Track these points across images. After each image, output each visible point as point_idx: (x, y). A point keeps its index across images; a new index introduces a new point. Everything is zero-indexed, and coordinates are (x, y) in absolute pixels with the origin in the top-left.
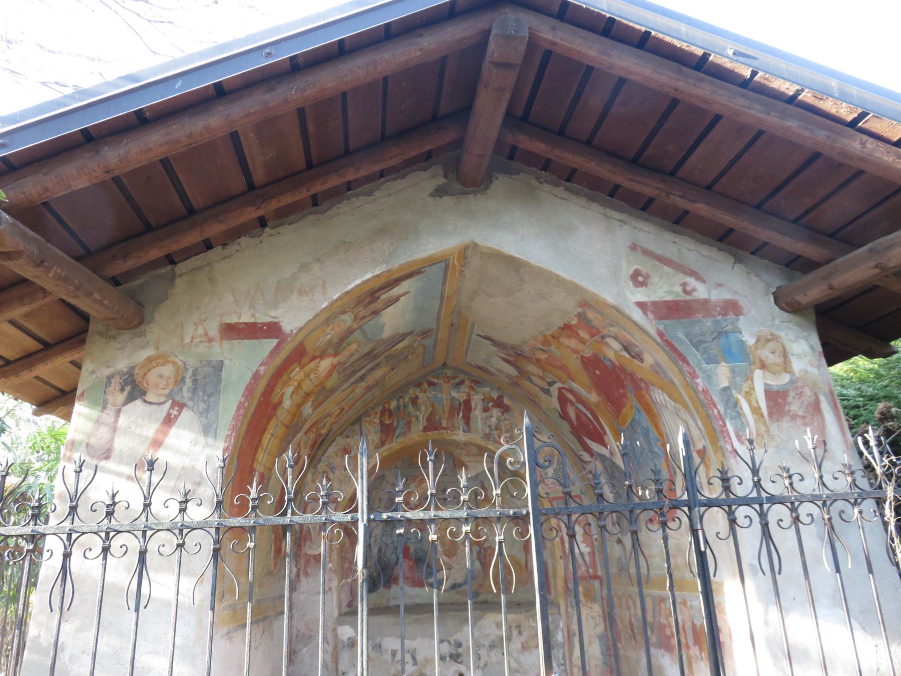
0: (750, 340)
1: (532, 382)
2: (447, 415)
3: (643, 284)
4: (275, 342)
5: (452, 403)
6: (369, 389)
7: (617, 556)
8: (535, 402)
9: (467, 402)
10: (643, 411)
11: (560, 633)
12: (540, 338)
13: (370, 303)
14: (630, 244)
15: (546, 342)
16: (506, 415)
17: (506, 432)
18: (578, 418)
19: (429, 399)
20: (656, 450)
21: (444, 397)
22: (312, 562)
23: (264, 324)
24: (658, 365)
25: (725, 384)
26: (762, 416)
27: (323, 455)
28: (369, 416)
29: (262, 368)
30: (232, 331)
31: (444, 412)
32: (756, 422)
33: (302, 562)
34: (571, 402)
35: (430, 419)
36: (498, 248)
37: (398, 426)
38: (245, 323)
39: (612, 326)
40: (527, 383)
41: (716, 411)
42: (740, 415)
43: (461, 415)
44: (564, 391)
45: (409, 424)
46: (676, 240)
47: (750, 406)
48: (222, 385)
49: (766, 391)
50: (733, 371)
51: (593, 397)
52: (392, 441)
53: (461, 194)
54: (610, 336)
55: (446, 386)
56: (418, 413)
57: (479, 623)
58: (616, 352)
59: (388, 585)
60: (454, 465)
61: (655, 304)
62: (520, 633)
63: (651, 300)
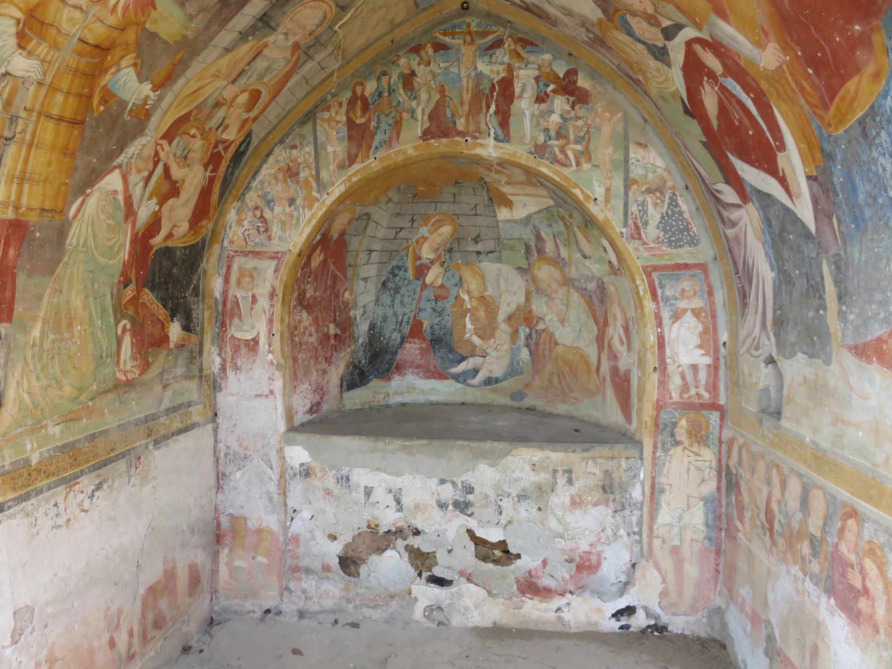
1: (630, 33)
2: (466, 107)
5: (478, 85)
6: (302, 52)
7: (761, 385)
8: (637, 82)
11: (638, 487)
16: (581, 111)
17: (577, 142)
19: (434, 76)
21: (463, 74)
22: (244, 350)
27: (253, 178)
28: (328, 109)
33: (228, 349)
34: (711, 75)
35: (435, 115)
37: (378, 127)
43: (493, 108)
44: (697, 48)
45: (397, 124)
51: (768, 57)
55: (468, 51)
57: (504, 461)
59: (385, 374)
60: (491, 199)
62: (570, 481)
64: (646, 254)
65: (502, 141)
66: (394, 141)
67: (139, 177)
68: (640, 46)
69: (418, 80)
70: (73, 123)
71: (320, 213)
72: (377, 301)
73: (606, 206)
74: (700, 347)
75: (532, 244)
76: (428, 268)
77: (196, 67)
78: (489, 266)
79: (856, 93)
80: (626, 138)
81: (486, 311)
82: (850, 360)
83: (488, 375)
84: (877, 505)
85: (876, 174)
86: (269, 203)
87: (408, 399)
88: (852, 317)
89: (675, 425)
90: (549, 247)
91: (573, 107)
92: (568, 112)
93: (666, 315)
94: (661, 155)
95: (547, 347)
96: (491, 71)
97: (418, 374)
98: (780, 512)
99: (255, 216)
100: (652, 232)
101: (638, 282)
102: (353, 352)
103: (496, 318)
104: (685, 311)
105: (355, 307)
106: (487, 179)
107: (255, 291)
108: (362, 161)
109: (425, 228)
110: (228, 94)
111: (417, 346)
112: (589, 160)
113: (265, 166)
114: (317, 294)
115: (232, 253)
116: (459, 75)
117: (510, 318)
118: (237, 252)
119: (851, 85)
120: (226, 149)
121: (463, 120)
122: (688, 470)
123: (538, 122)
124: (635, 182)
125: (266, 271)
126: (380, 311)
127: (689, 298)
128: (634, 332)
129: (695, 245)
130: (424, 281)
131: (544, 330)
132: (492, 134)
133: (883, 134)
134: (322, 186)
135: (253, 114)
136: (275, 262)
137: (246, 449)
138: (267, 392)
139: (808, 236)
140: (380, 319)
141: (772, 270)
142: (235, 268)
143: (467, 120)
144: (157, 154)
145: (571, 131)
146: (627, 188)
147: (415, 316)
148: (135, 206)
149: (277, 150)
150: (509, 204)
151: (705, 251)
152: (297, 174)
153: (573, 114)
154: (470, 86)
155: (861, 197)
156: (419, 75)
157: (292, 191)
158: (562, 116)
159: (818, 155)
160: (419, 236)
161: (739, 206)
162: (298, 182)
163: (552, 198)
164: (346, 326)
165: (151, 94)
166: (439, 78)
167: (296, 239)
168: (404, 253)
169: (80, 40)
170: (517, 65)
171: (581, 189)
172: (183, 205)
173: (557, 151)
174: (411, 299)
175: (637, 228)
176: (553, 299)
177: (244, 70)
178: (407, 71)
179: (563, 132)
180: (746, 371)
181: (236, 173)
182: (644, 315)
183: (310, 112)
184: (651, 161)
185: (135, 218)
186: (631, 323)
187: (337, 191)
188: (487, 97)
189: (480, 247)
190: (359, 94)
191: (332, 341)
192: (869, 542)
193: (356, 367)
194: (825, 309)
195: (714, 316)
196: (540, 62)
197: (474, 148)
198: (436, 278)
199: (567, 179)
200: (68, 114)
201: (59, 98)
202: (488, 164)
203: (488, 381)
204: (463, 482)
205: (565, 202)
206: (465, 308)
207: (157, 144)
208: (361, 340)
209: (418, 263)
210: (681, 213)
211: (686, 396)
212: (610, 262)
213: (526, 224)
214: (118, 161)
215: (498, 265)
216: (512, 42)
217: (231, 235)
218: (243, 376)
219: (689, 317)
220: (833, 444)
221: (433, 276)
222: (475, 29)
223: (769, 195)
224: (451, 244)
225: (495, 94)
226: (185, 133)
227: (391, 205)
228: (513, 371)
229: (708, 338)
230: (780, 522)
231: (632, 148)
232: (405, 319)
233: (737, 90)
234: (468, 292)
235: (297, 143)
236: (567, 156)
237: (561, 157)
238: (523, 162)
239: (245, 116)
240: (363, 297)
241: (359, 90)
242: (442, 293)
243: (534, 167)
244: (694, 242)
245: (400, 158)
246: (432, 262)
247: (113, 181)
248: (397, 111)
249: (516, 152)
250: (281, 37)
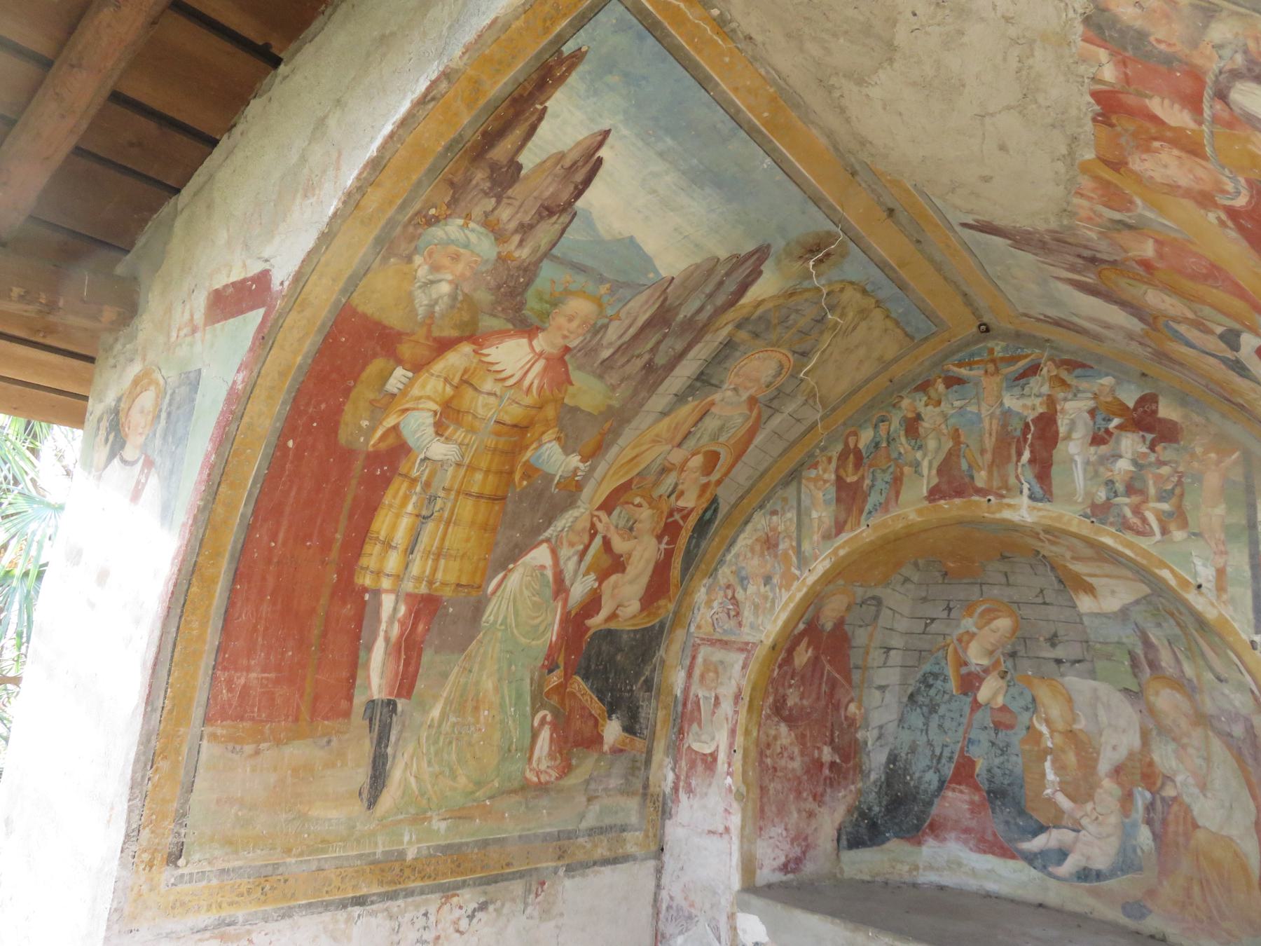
2: (988, 457)
5: (1004, 426)
6: (764, 406)
8: (1242, 407)
16: (1166, 452)
17: (1161, 499)
19: (946, 417)
21: (984, 413)
22: (700, 767)
27: (728, 550)
28: (815, 466)
29: (240, 377)
31: (983, 452)
33: (683, 763)
35: (945, 468)
37: (873, 486)
43: (1026, 455)
45: (897, 481)
52: (859, 524)
55: (991, 384)
56: (919, 455)
60: (1061, 581)
65: (1041, 500)
67: (572, 551)
69: (926, 425)
70: (493, 499)
71: (799, 595)
72: (901, 720)
73: (1219, 597)
76: (981, 680)
77: (628, 435)
78: (1075, 682)
81: (1077, 755)
83: (1083, 863)
86: (743, 580)
87: (948, 879)
90: (1165, 659)
91: (1152, 448)
92: (1145, 455)
95: (1181, 829)
96: (1024, 406)
97: (966, 842)
99: (726, 596)
102: (860, 792)
103: (1094, 768)
105: (867, 727)
106: (1043, 552)
108: (852, 530)
109: (970, 621)
110: (677, 456)
111: (966, 797)
112: (1184, 524)
113: (742, 536)
114: (805, 702)
116: (979, 415)
117: (1117, 771)
118: (703, 639)
120: (685, 518)
121: (983, 474)
123: (1096, 472)
130: (975, 700)
131: (1175, 799)
132: (1026, 491)
134: (803, 561)
135: (715, 477)
136: (743, 656)
138: (721, 829)
140: (906, 749)
142: (700, 660)
143: (990, 473)
144: (593, 526)
145: (1151, 482)
147: (962, 749)
148: (567, 582)
149: (756, 516)
150: (1090, 590)
152: (776, 545)
153: (1153, 458)
154: (994, 427)
156: (926, 418)
157: (769, 566)
158: (1135, 462)
160: (961, 631)
162: (776, 556)
164: (850, 753)
165: (581, 465)
166: (952, 421)
168: (940, 653)
169: (497, 422)
171: (1172, 571)
172: (631, 582)
174: (955, 724)
176: (1184, 747)
177: (690, 432)
178: (910, 415)
179: (1137, 485)
181: (703, 545)
185: (568, 595)
187: (821, 566)
188: (1018, 441)
190: (852, 446)
191: (826, 772)
193: (863, 815)
196: (1095, 389)
197: (1000, 511)
198: (995, 696)
199: (1146, 554)
200: (488, 490)
201: (479, 476)
203: (1085, 875)
206: (1043, 746)
207: (593, 516)
208: (873, 777)
209: (964, 670)
214: (547, 534)
216: (1053, 367)
217: (698, 619)
218: (696, 802)
221: (989, 690)
222: (1001, 355)
224: (1013, 645)
225: (1029, 436)
226: (627, 503)
228: (1126, 863)
232: (946, 753)
234: (1048, 722)
235: (778, 508)
236: (1144, 520)
237: (1134, 520)
239: (704, 480)
240: (877, 713)
241: (852, 441)
242: (1005, 718)
245: (900, 525)
246: (986, 671)
247: (540, 555)
248: (897, 466)
249: (1060, 517)
250: (729, 393)
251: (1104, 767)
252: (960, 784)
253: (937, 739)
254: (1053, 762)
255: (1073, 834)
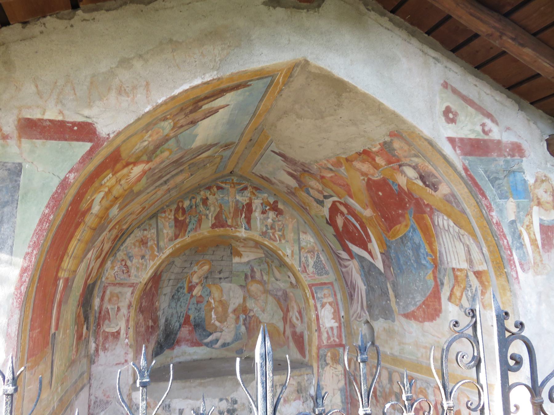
0: (531, 181)
1: (308, 193)
2: (232, 215)
3: (452, 121)
4: (88, 146)
5: (237, 205)
8: (306, 209)
9: (249, 205)
10: (419, 231)
11: (313, 388)
12: (334, 159)
13: (191, 112)
14: (442, 82)
15: (338, 163)
16: (280, 218)
17: (279, 231)
18: (345, 225)
19: (217, 200)
20: (424, 262)
22: (110, 338)
23: (74, 124)
24: (453, 195)
25: (513, 218)
26: (538, 247)
27: (122, 245)
28: (165, 212)
29: (72, 176)
30: (32, 128)
31: (230, 213)
32: (533, 252)
33: (101, 338)
34: (342, 213)
36: (329, 69)
37: (190, 222)
38: (50, 121)
39: (416, 156)
40: (304, 194)
41: (505, 241)
42: (522, 245)
43: (244, 215)
44: (338, 204)
45: (200, 221)
46: (477, 83)
47: (530, 238)
48: (21, 192)
49: (540, 225)
50: (518, 206)
51: (368, 213)
53: (294, 7)
54: (410, 166)
56: (208, 212)
58: (409, 180)
59: (171, 346)
60: (231, 253)
61: (461, 140)
63: (459, 136)
64: (309, 279)
65: (248, 230)
66: (198, 229)
68: (311, 198)
74: (333, 319)
75: (249, 274)
76: (195, 287)
78: (225, 285)
79: (399, 230)
80: (298, 230)
82: (403, 320)
84: (421, 373)
85: (407, 255)
88: (401, 304)
89: (326, 355)
90: (258, 275)
91: (277, 216)
93: (319, 306)
94: (312, 237)
97: (187, 345)
98: (379, 386)
99: (121, 264)
100: (311, 269)
101: (307, 291)
102: (158, 335)
103: (227, 311)
104: (326, 303)
106: (233, 245)
107: (119, 305)
112: (284, 239)
113: (129, 239)
115: (107, 285)
116: (228, 200)
117: (235, 311)
119: (398, 227)
122: (333, 376)
124: (303, 248)
125: (126, 293)
126: (170, 311)
127: (327, 297)
128: (304, 314)
129: (328, 274)
132: (243, 227)
133: (409, 243)
134: (160, 249)
136: (132, 289)
137: (108, 397)
138: (123, 361)
139: (381, 273)
140: (170, 316)
141: (365, 285)
142: (108, 292)
146: (300, 250)
150: (240, 255)
151: (331, 277)
152: (147, 243)
153: (277, 219)
155: (402, 262)
157: (143, 252)
158: (273, 220)
159: (385, 246)
160: (193, 271)
161: (349, 260)
162: (147, 247)
163: (264, 254)
164: (156, 320)
166: (219, 201)
167: (144, 276)
168: (184, 280)
170: (253, 198)
173: (271, 235)
175: (305, 268)
176: (258, 300)
178: (204, 197)
179: (273, 227)
180: (355, 328)
182: (310, 306)
183: (155, 213)
184: (308, 239)
186: (302, 310)
187: (168, 252)
189: (221, 276)
190: (181, 206)
191: (150, 330)
192: (420, 388)
194: (390, 301)
195: (337, 304)
198: (198, 292)
199: (275, 246)
202: (237, 239)
203: (224, 345)
204: (231, 399)
205: (272, 256)
209: (190, 285)
210: (321, 261)
211: (329, 341)
212: (291, 282)
213: (247, 265)
215: (230, 284)
217: (107, 274)
218: (108, 354)
219: (328, 306)
220: (400, 353)
223: (364, 257)
227: (184, 256)
228: (237, 338)
229: (336, 315)
230: (379, 391)
231: (301, 234)
233: (353, 220)
234: (214, 299)
235: (147, 228)
236: (275, 237)
237: (273, 237)
238: (257, 239)
240: (163, 303)
243: (262, 241)
244: (327, 273)
245: (201, 236)
246: (197, 284)
248: (200, 215)
251: (230, 310)
252: (185, 324)
253: (179, 309)
254: (214, 312)
255: (220, 333)
